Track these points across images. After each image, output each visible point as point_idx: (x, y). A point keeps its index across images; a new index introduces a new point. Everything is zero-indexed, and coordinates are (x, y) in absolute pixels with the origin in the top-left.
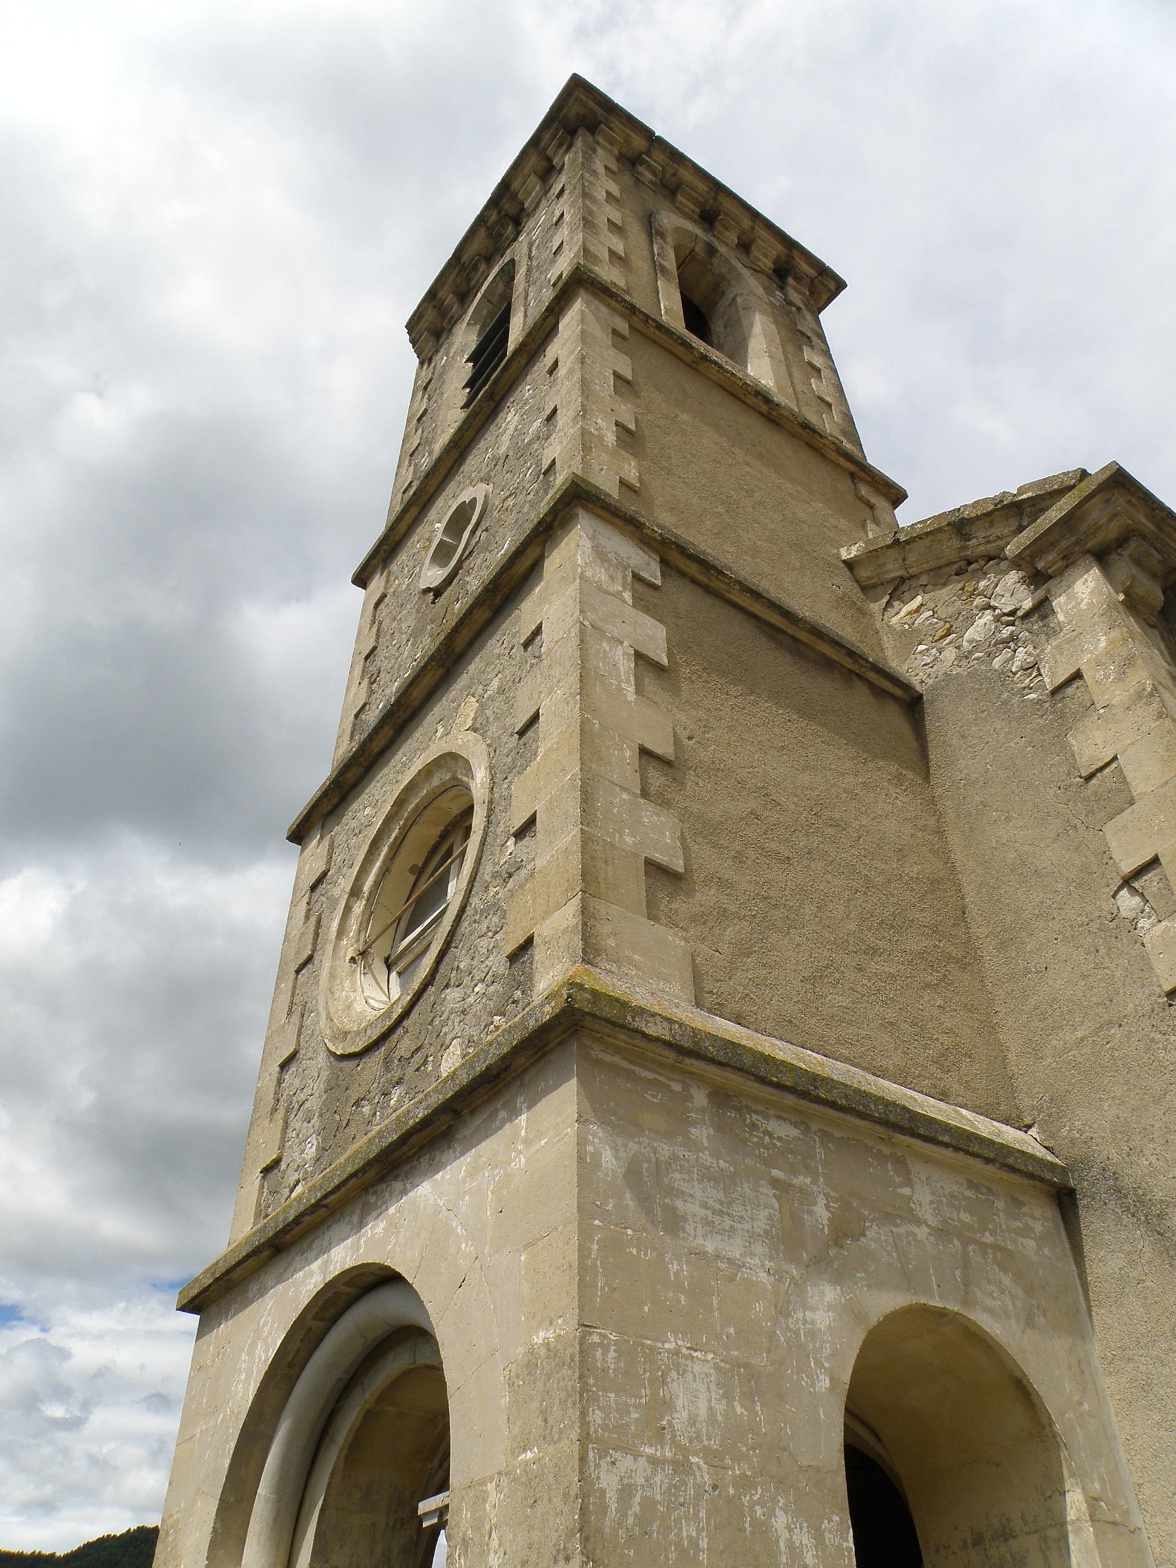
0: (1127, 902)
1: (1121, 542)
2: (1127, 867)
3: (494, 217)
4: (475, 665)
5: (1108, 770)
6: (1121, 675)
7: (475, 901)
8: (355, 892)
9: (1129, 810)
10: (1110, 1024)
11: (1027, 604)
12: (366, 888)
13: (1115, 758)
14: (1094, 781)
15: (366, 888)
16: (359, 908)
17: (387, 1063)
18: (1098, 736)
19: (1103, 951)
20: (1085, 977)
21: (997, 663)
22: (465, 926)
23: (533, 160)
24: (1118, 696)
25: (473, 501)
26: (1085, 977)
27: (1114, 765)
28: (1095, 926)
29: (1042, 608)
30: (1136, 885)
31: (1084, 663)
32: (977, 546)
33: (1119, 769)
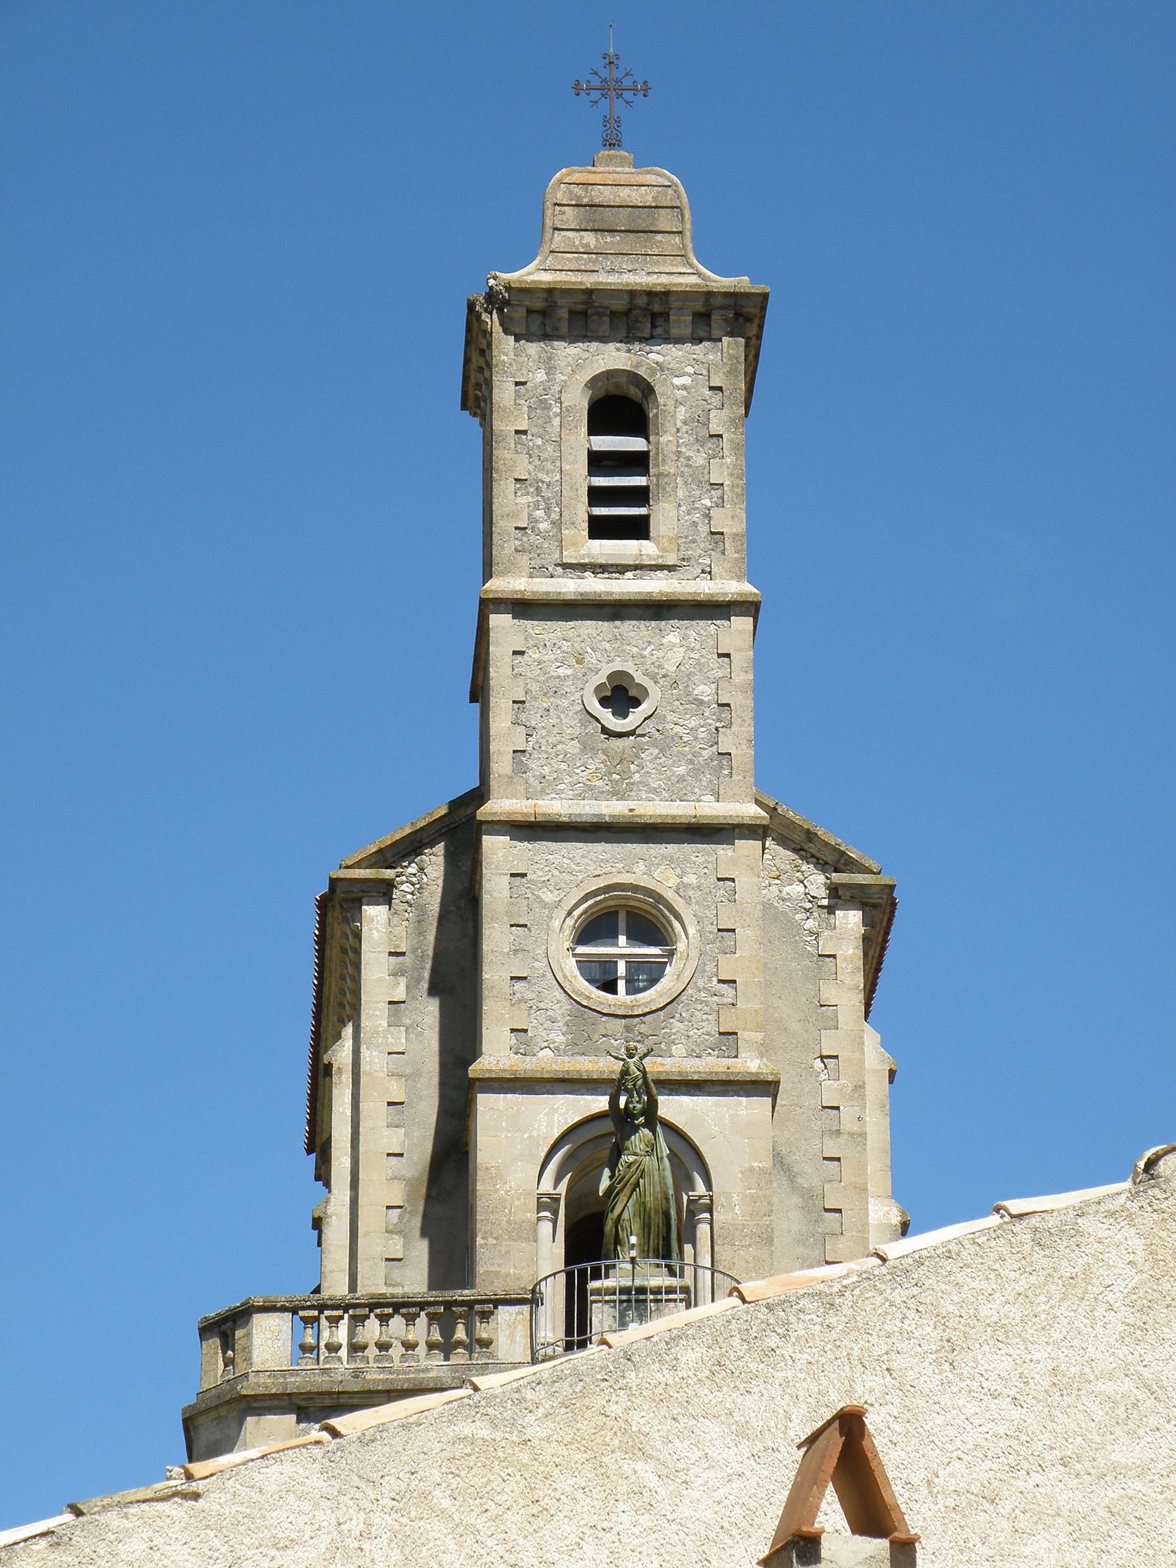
0: (818, 1064)
1: (874, 906)
2: (825, 1053)
3: (642, 301)
4: (672, 848)
5: (831, 1008)
6: (852, 973)
7: (690, 991)
8: (569, 913)
9: (832, 1031)
10: (797, 1105)
11: (825, 902)
12: (577, 913)
13: (836, 1006)
14: (824, 1008)
15: (577, 913)
16: (570, 922)
17: (628, 1029)
18: (833, 991)
19: (803, 1077)
20: (793, 1083)
21: (798, 917)
22: (683, 998)
23: (699, 307)
24: (848, 981)
25: (645, 692)
26: (793, 1083)
27: (835, 1008)
28: (803, 1066)
29: (831, 909)
30: (825, 1060)
31: (839, 954)
32: (810, 846)
33: (837, 1011)
